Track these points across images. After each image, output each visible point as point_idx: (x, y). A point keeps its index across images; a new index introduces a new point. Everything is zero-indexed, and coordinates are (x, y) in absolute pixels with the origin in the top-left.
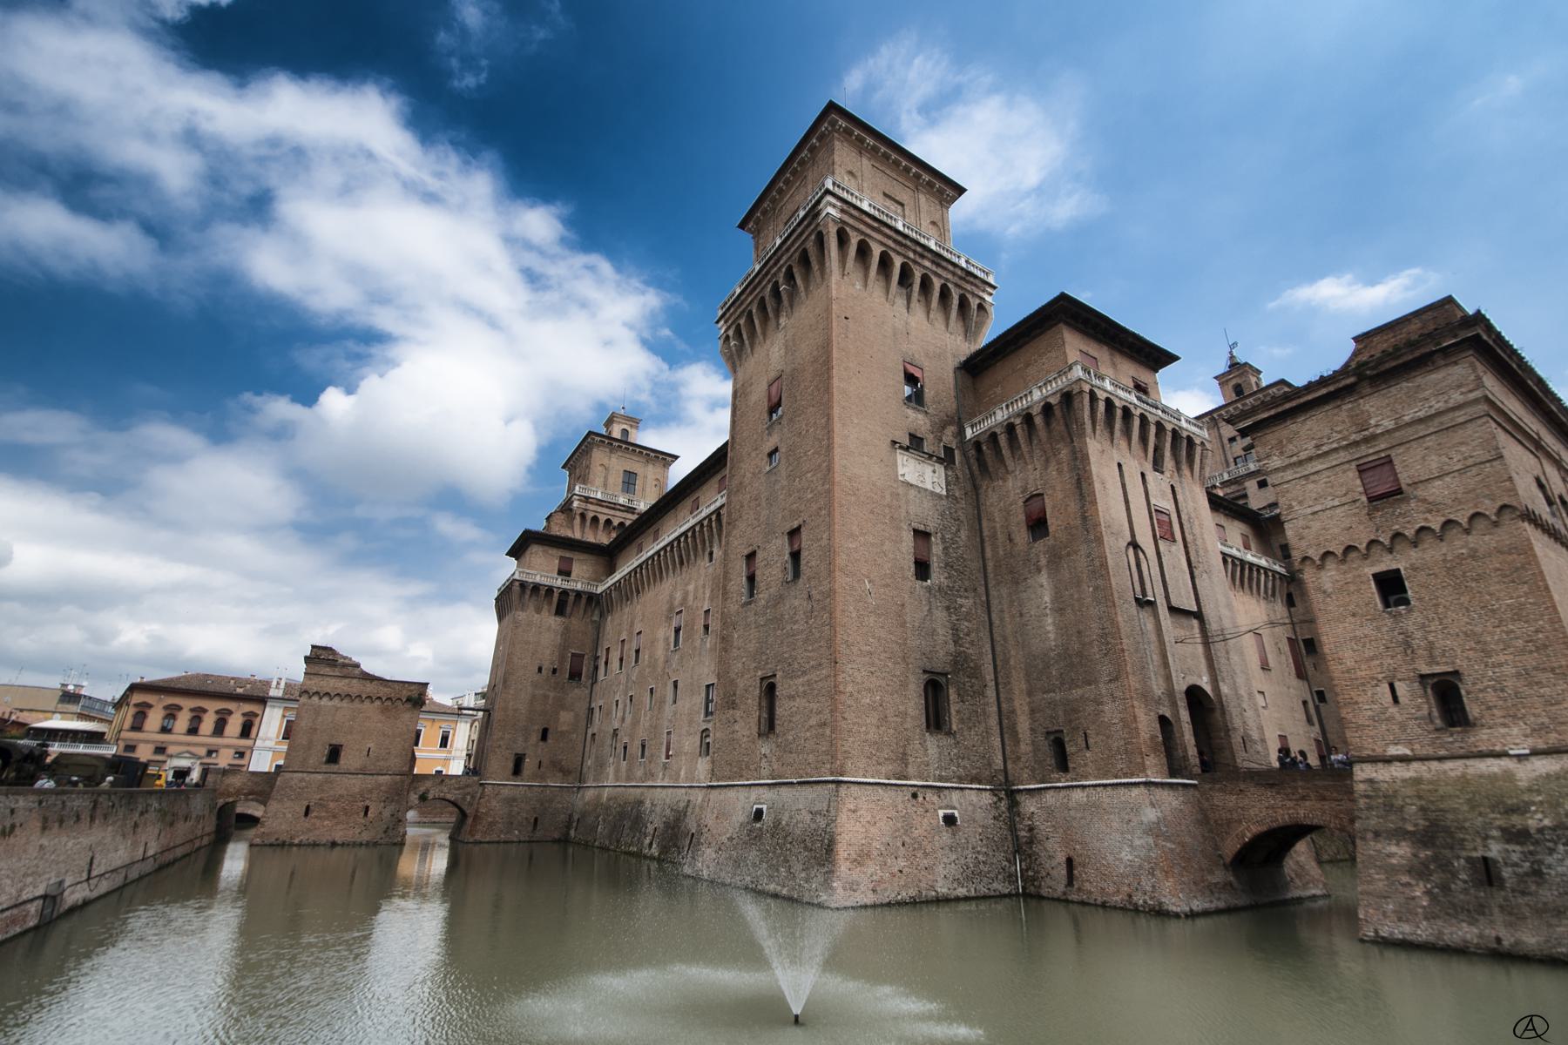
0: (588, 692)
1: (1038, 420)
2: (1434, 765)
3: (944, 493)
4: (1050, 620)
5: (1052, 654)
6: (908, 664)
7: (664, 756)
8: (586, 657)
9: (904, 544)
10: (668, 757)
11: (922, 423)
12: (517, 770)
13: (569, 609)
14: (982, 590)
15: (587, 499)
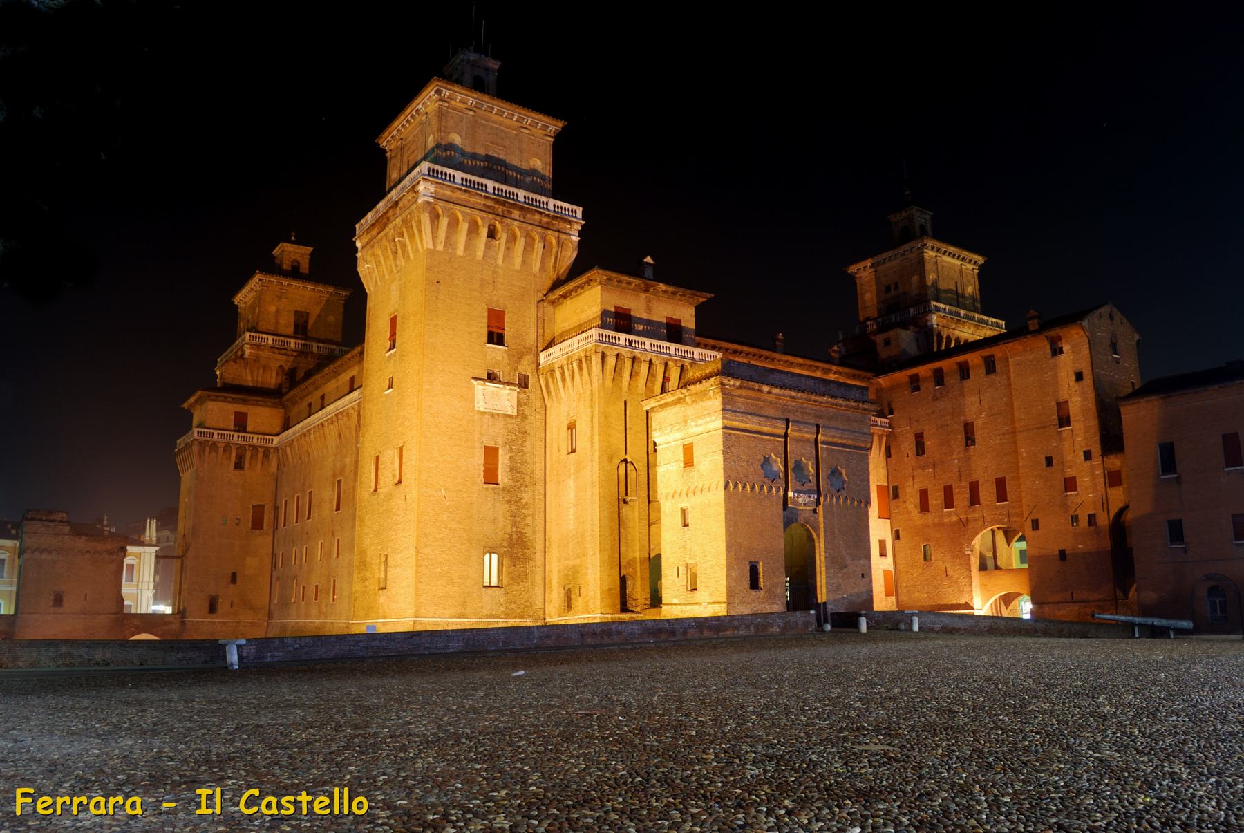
0: (270, 538)
1: (575, 365)
2: (684, 607)
3: (515, 414)
4: (572, 511)
5: (571, 535)
6: (472, 544)
7: (331, 599)
8: (266, 507)
9: (476, 458)
10: (334, 600)
11: (500, 358)
12: (212, 609)
13: (247, 465)
14: (540, 485)
15: (259, 347)
